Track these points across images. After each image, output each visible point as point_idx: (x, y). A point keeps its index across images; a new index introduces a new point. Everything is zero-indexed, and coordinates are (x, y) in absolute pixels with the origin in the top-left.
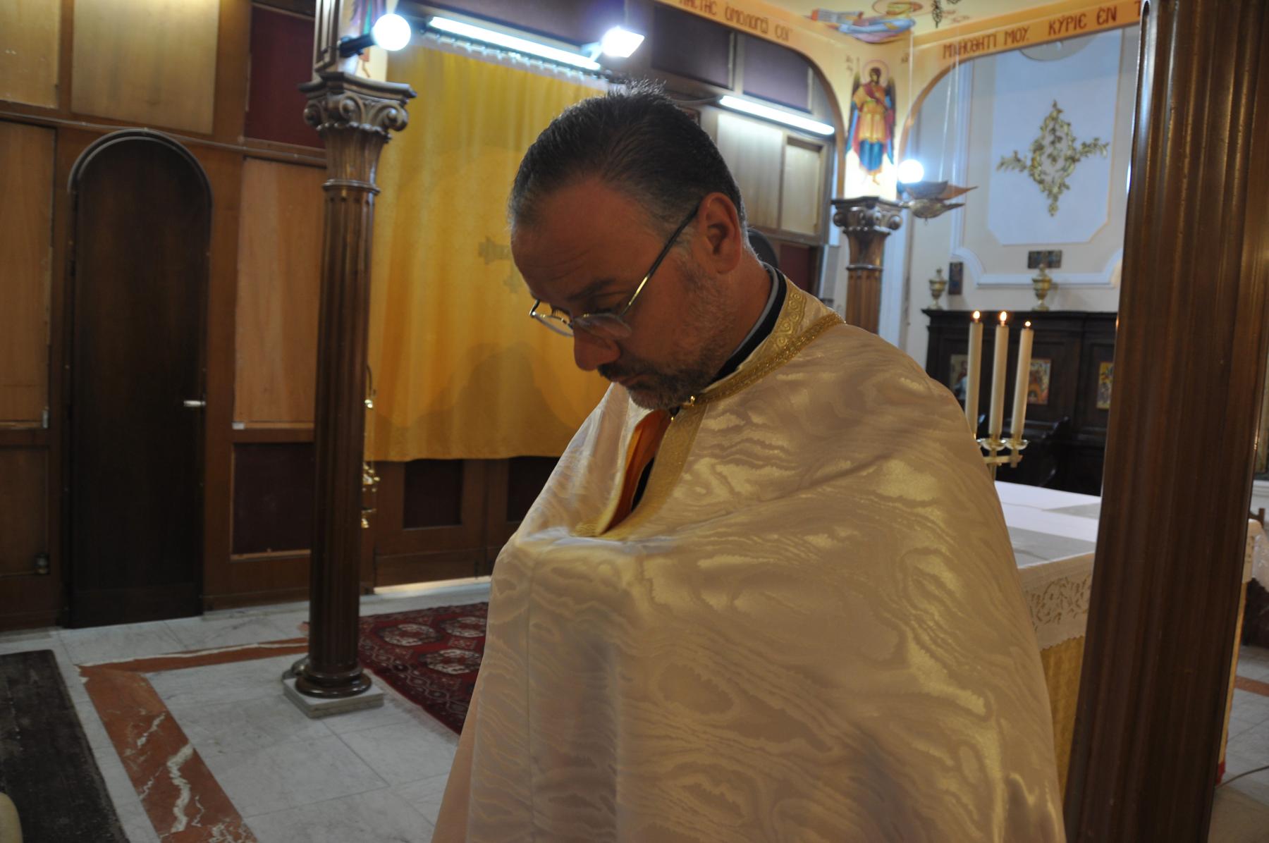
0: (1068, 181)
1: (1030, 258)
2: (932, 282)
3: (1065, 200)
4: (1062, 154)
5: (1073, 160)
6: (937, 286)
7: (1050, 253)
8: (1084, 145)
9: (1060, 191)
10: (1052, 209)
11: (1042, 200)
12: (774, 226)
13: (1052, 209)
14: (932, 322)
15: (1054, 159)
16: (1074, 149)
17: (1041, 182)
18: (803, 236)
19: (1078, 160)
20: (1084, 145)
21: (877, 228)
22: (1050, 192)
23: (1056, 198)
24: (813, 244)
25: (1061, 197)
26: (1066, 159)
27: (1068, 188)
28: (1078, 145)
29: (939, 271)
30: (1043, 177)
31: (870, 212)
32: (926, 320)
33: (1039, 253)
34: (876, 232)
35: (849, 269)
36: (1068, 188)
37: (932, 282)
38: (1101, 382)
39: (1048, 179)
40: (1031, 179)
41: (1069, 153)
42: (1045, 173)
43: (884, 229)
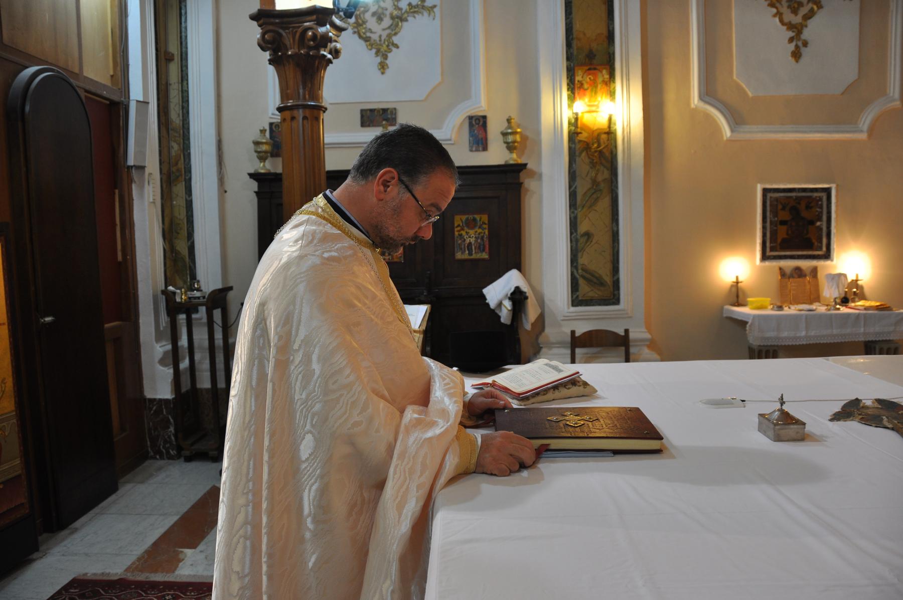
0: (395, 39)
1: (362, 116)
2: (257, 143)
3: (394, 58)
4: (388, 13)
5: (402, 19)
6: (264, 148)
7: (385, 111)
8: (410, 4)
9: (390, 51)
10: (383, 67)
11: (370, 59)
12: (76, 70)
13: (383, 67)
14: (259, 187)
15: (380, 19)
16: (400, 9)
17: (367, 40)
18: (105, 86)
19: (407, 20)
20: (410, 4)
21: (322, 52)
22: (378, 53)
23: (385, 57)
24: (115, 98)
25: (389, 55)
26: (392, 18)
27: (397, 47)
28: (403, 5)
29: (263, 131)
30: (368, 34)
31: (322, 30)
32: (254, 185)
33: (372, 111)
34: (324, 56)
35: (280, 109)
36: (397, 47)
37: (257, 143)
38: (456, 233)
39: (375, 37)
40: (356, 36)
41: (395, 13)
42: (371, 31)
43: (329, 56)
